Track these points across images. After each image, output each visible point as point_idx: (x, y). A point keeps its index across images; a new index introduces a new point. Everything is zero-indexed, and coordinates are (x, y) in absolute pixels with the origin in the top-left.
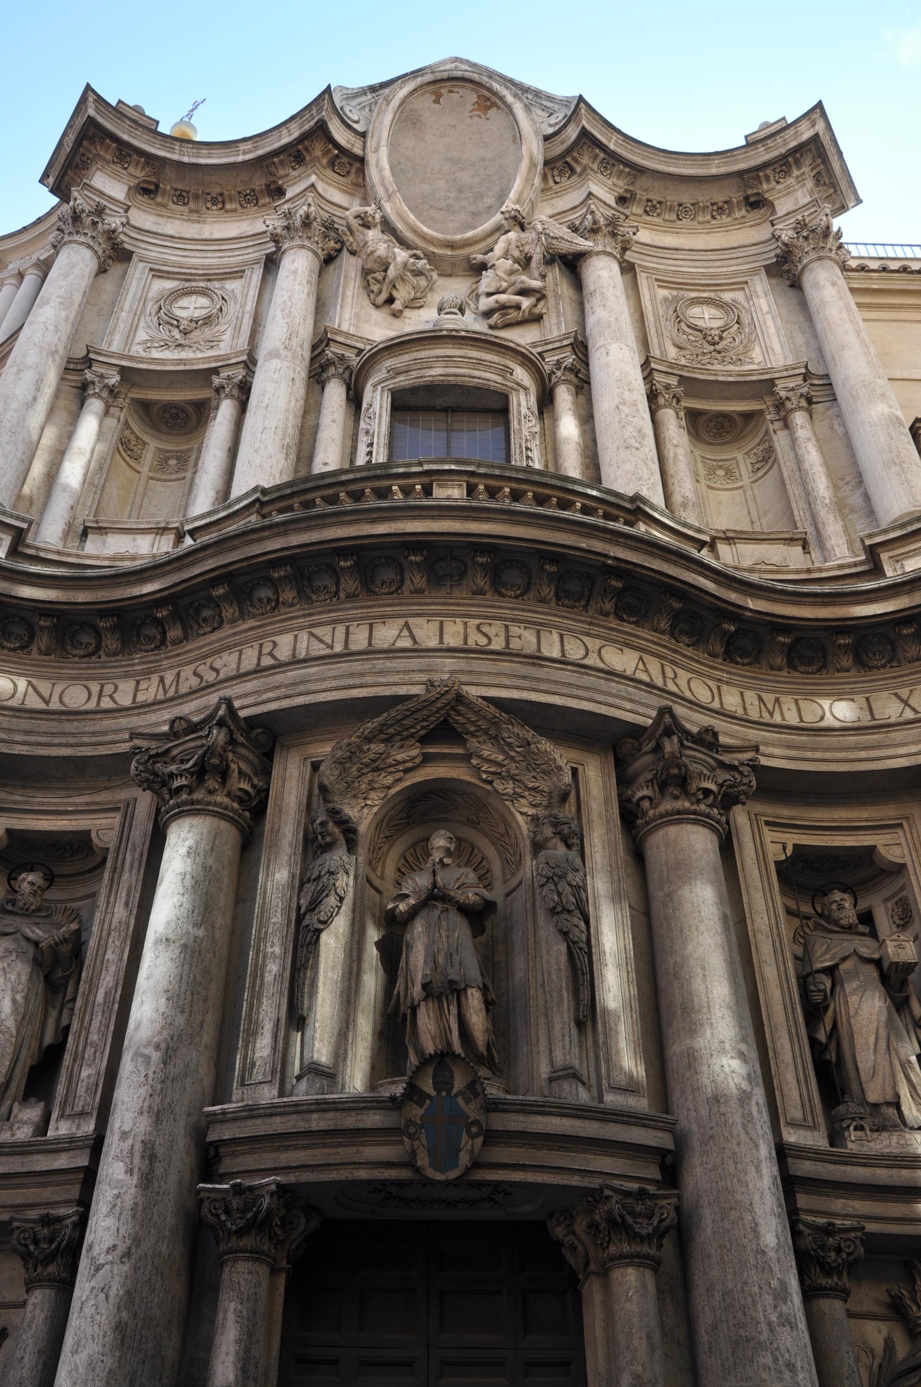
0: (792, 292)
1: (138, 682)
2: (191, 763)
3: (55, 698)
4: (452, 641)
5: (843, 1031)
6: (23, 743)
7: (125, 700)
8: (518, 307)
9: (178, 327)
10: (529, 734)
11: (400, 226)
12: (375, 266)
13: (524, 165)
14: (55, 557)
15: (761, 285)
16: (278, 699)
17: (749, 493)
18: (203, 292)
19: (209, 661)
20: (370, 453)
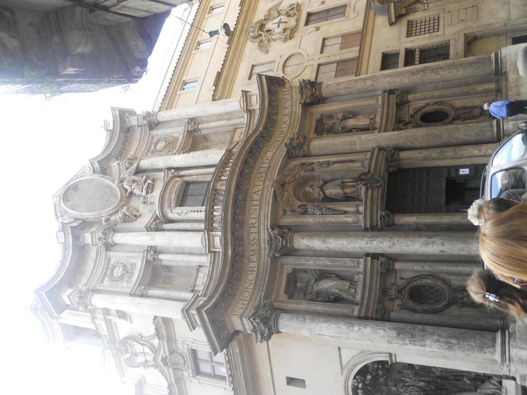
0: (159, 126)
1: (250, 262)
2: (281, 239)
3: (251, 282)
4: (261, 183)
5: (355, 127)
6: (263, 286)
7: (256, 264)
8: (149, 184)
9: (124, 275)
10: (286, 169)
11: (111, 212)
12: (124, 218)
13: (101, 179)
14: (205, 291)
15: (154, 133)
16: (267, 220)
17: (213, 143)
18: (113, 268)
19: (250, 242)
20: (194, 211)
